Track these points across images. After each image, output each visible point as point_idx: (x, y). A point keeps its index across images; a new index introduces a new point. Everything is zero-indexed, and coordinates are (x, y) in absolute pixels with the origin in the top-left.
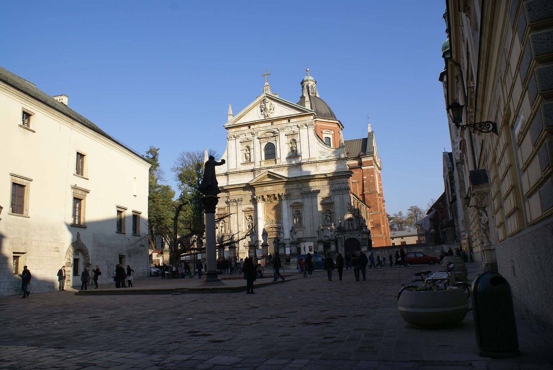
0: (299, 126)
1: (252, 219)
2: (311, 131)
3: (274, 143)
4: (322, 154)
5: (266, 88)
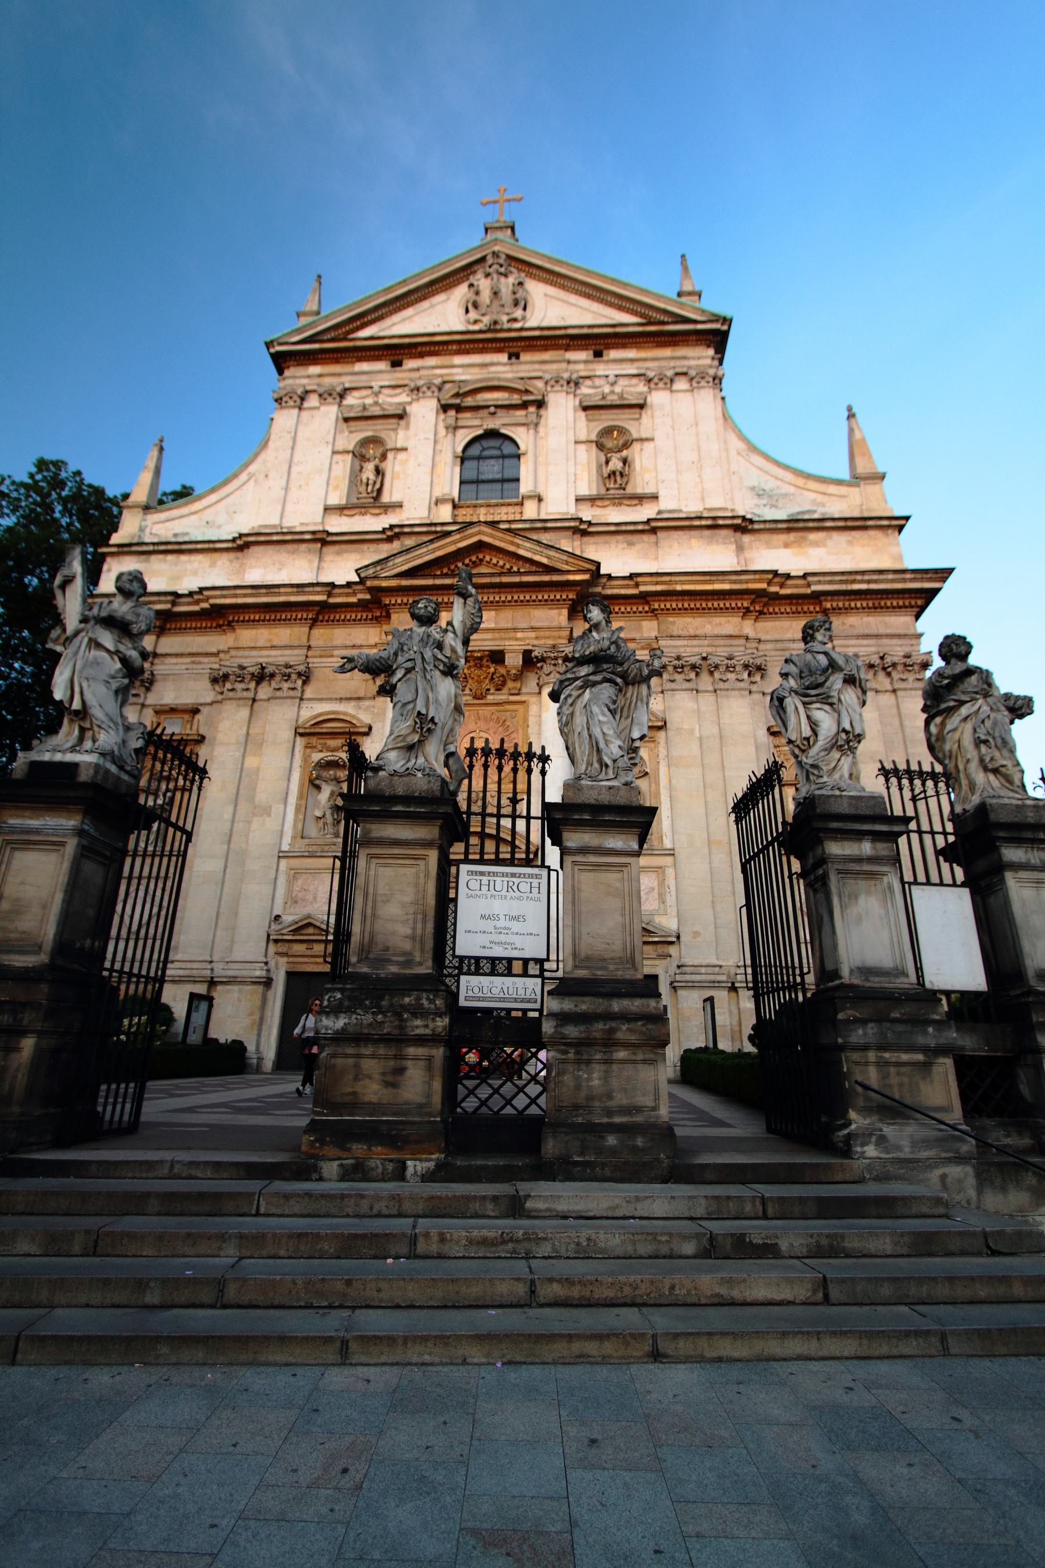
0: (651, 374)
4: (764, 502)
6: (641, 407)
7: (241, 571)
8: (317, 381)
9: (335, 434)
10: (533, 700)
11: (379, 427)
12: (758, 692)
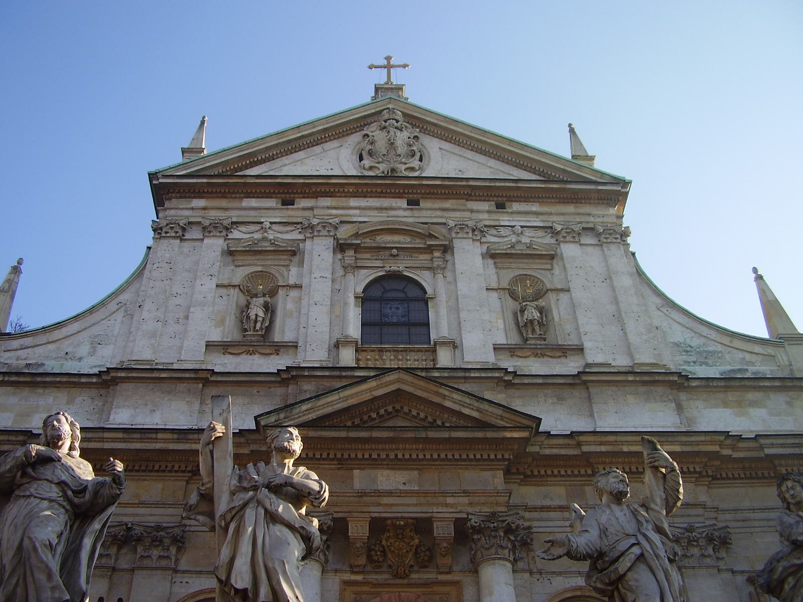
0: (559, 228)
3: (425, 279)
7: (105, 411)
8: (201, 213)
9: (220, 267)
10: (467, 580)
11: (269, 263)
12: (727, 570)
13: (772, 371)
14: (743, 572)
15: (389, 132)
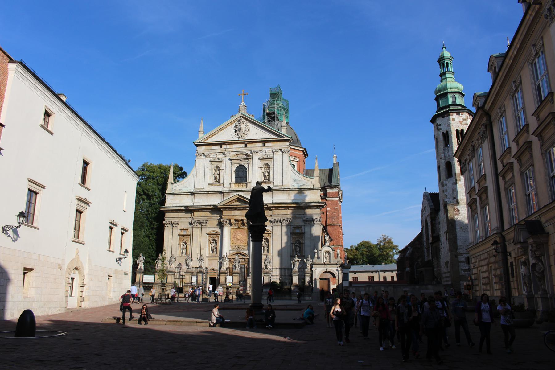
0: (274, 151)
1: (216, 243)
2: (286, 156)
3: (246, 166)
5: (243, 107)
6: (272, 159)
7: (193, 199)
13: (310, 185)
14: (293, 226)
15: (240, 125)
